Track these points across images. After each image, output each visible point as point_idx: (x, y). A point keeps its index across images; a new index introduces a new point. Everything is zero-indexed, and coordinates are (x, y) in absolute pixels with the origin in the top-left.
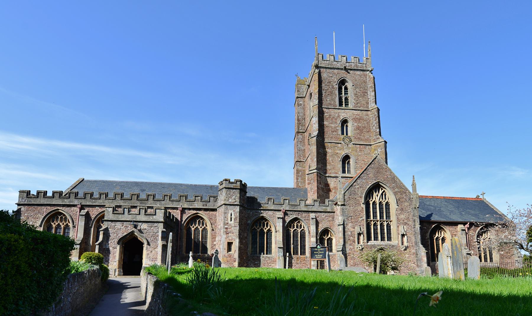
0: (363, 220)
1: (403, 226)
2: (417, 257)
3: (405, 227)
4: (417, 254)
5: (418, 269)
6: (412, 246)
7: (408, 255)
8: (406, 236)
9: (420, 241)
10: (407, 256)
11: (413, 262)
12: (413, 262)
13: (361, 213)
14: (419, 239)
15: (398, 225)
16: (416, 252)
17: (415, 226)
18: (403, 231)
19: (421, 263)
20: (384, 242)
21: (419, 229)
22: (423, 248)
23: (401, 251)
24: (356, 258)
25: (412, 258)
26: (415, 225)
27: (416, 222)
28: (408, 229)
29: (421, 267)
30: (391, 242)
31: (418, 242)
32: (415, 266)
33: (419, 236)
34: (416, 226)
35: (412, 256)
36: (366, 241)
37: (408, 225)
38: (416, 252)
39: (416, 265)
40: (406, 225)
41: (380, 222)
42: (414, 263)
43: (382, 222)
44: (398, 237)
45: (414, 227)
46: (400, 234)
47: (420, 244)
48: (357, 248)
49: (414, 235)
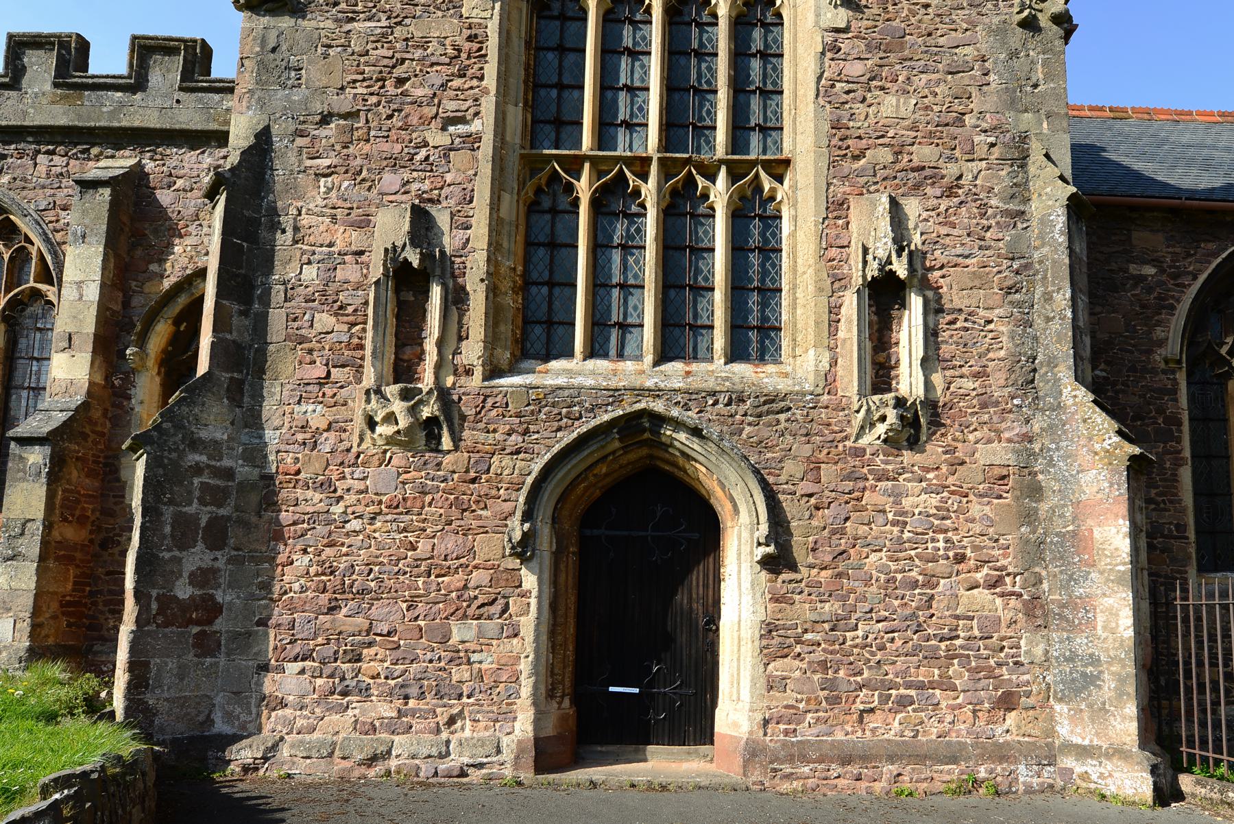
0: (472, 141)
1: (885, 200)
2: (1029, 517)
3: (912, 208)
4: (1035, 491)
5: (1039, 651)
6: (984, 406)
7: (934, 500)
8: (916, 302)
9: (1064, 350)
10: (919, 501)
11: (979, 576)
12: (979, 576)
13: (457, 83)
14: (1055, 326)
15: (840, 189)
16: (1026, 469)
17: (1027, 200)
18: (883, 246)
19: (1065, 587)
20: (694, 367)
21: (1060, 219)
22: (1103, 422)
23: (859, 453)
24: (355, 525)
25: (977, 528)
26: (1020, 191)
27: (1036, 157)
28: (944, 230)
29: (1072, 627)
30: (771, 368)
31: (1052, 363)
32: (1006, 616)
33: (1063, 297)
34: (1034, 205)
35: (977, 509)
36: (472, 352)
37: (950, 192)
38: (1026, 469)
39: (1013, 602)
40: (929, 190)
41: (668, 169)
42: (994, 584)
43: (690, 182)
44: (834, 311)
45: (1006, 213)
46: (857, 281)
47: (1065, 373)
48: (371, 424)
49: (1010, 290)
